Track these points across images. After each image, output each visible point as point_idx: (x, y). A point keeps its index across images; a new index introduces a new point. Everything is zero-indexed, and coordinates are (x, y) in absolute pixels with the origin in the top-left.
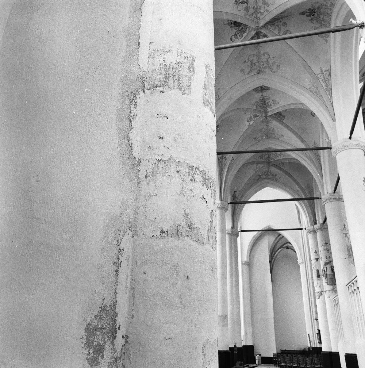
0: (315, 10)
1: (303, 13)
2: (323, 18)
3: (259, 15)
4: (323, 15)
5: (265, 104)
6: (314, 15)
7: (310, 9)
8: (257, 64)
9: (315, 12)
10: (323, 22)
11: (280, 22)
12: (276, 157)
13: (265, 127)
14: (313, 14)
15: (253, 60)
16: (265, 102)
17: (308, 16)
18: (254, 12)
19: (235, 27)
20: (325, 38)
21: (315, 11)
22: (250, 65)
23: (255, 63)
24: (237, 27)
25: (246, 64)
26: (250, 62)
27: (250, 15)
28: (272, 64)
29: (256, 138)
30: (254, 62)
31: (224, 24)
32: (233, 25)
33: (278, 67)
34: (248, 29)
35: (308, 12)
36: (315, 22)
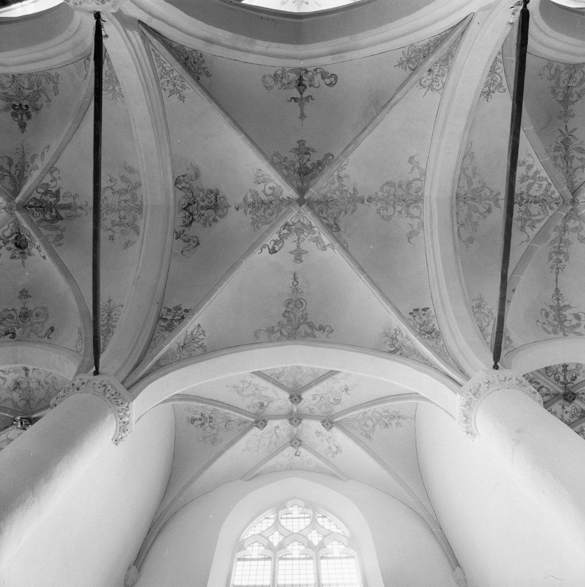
0: (14, 106)
1: (23, 126)
2: (27, 89)
5: (271, 202)
6: (26, 106)
7: (14, 115)
8: (122, 213)
10: (35, 89)
11: (28, 166)
12: (542, 179)
13: (373, 207)
14: (25, 108)
15: (113, 222)
16: (263, 203)
17: (29, 117)
19: (29, 247)
20: (56, 81)
21: (17, 104)
22: (123, 228)
23: (120, 218)
24: (29, 244)
25: (117, 236)
26: (116, 229)
28: (126, 182)
29: (410, 233)
30: (117, 220)
31: (24, 266)
32: (26, 251)
33: (131, 171)
36: (39, 103)
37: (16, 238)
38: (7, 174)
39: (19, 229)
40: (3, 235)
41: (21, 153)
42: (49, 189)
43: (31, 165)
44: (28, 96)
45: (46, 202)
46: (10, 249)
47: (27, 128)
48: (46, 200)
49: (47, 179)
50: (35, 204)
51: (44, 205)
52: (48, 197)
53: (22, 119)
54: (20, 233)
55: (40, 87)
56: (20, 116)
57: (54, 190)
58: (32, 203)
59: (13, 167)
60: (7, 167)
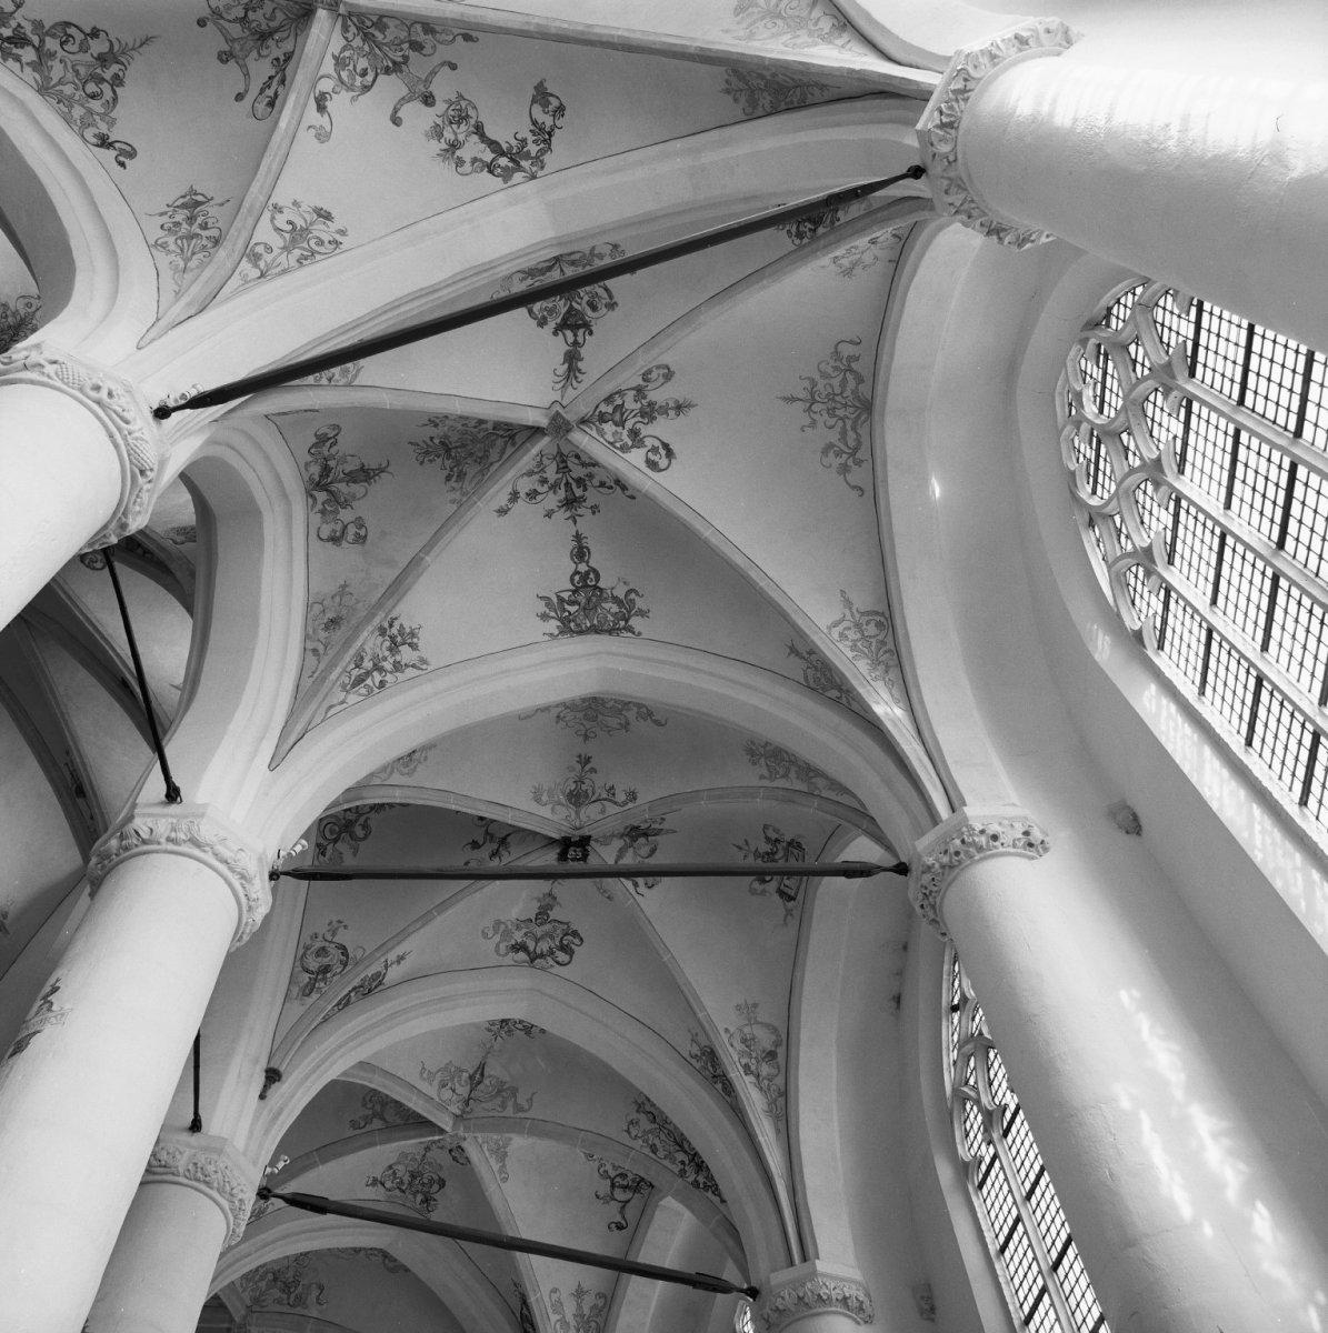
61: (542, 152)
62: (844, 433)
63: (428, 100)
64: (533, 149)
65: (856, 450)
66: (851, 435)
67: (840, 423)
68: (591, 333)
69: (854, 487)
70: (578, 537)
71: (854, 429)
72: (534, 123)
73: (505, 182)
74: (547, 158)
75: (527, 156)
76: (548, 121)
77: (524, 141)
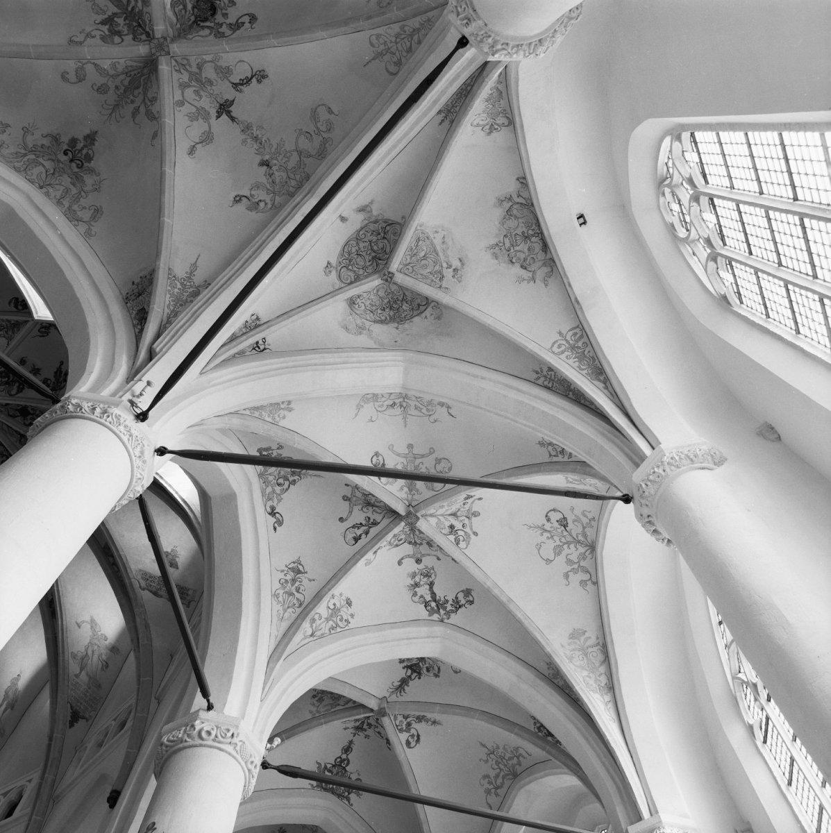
0: (80, 167)
1: (91, 138)
2: (44, 166)
3: (185, 77)
4: (52, 172)
6: (65, 153)
7: (89, 158)
9: (71, 161)
11: (117, 87)
14: (70, 153)
17: (74, 141)
18: (200, 74)
21: (74, 165)
27: (203, 65)
34: (174, 20)
35: (82, 149)
36: (46, 142)
37: (206, 20)
38: (147, 101)
39: (191, 27)
40: (210, 34)
41: (118, 114)
42: (107, 33)
43: (111, 84)
44: (53, 160)
45: (129, 26)
46: (225, 15)
47: (87, 132)
48: (126, 27)
49: (98, 41)
50: (142, 34)
51: (135, 24)
52: (120, 28)
53: (85, 146)
54: (194, 22)
55: (23, 151)
56: (84, 152)
57: (105, 28)
58: (144, 37)
59: (136, 105)
60: (142, 109)
61: (452, 611)
62: (497, 776)
63: (418, 561)
64: (449, 608)
65: (497, 788)
66: (499, 781)
67: (498, 770)
68: (420, 678)
69: (488, 804)
70: (351, 742)
71: (503, 778)
72: (457, 598)
73: (430, 615)
74: (453, 615)
75: (445, 609)
76: (463, 602)
77: (447, 601)
